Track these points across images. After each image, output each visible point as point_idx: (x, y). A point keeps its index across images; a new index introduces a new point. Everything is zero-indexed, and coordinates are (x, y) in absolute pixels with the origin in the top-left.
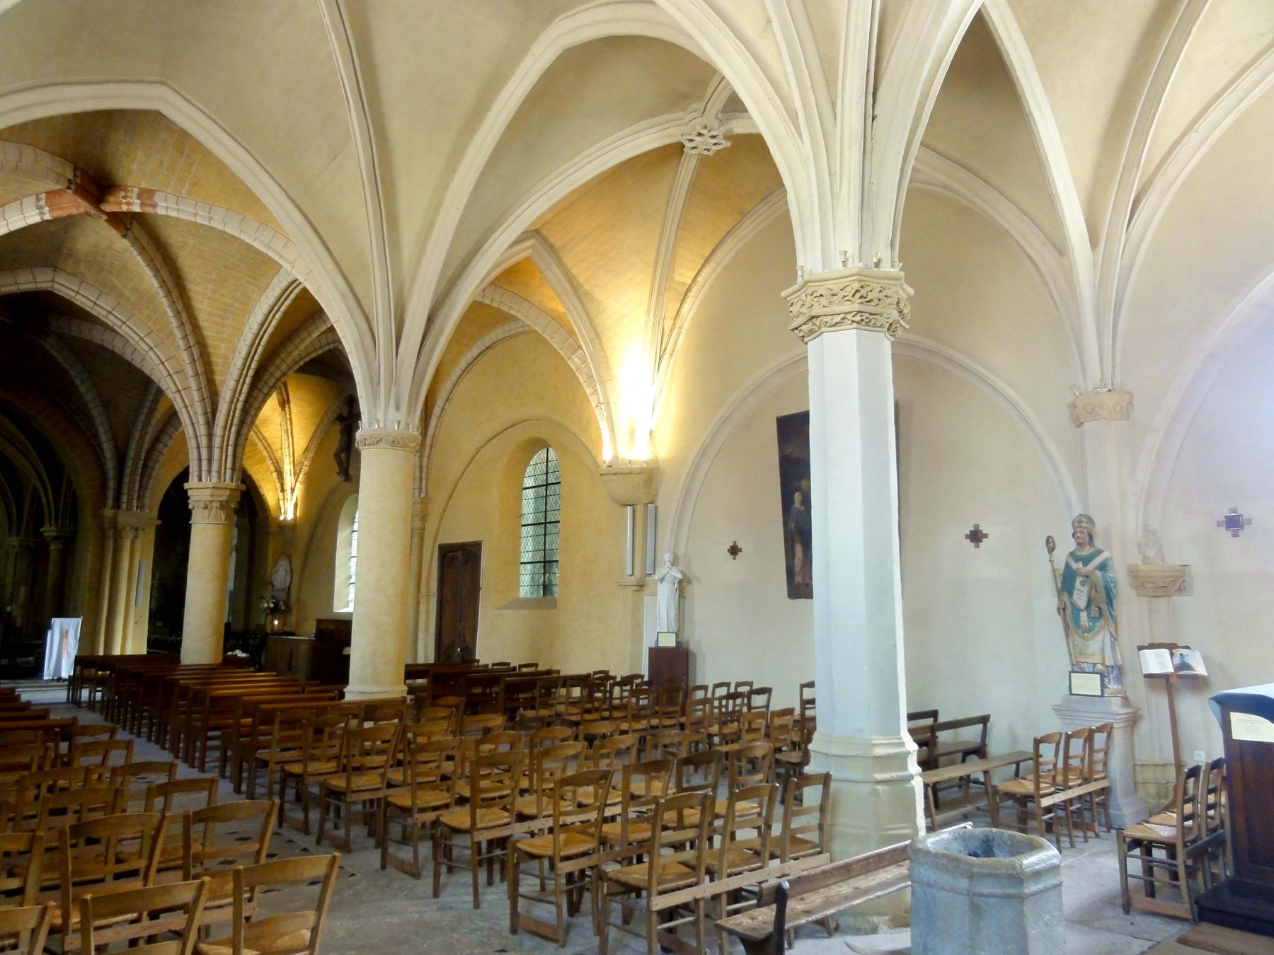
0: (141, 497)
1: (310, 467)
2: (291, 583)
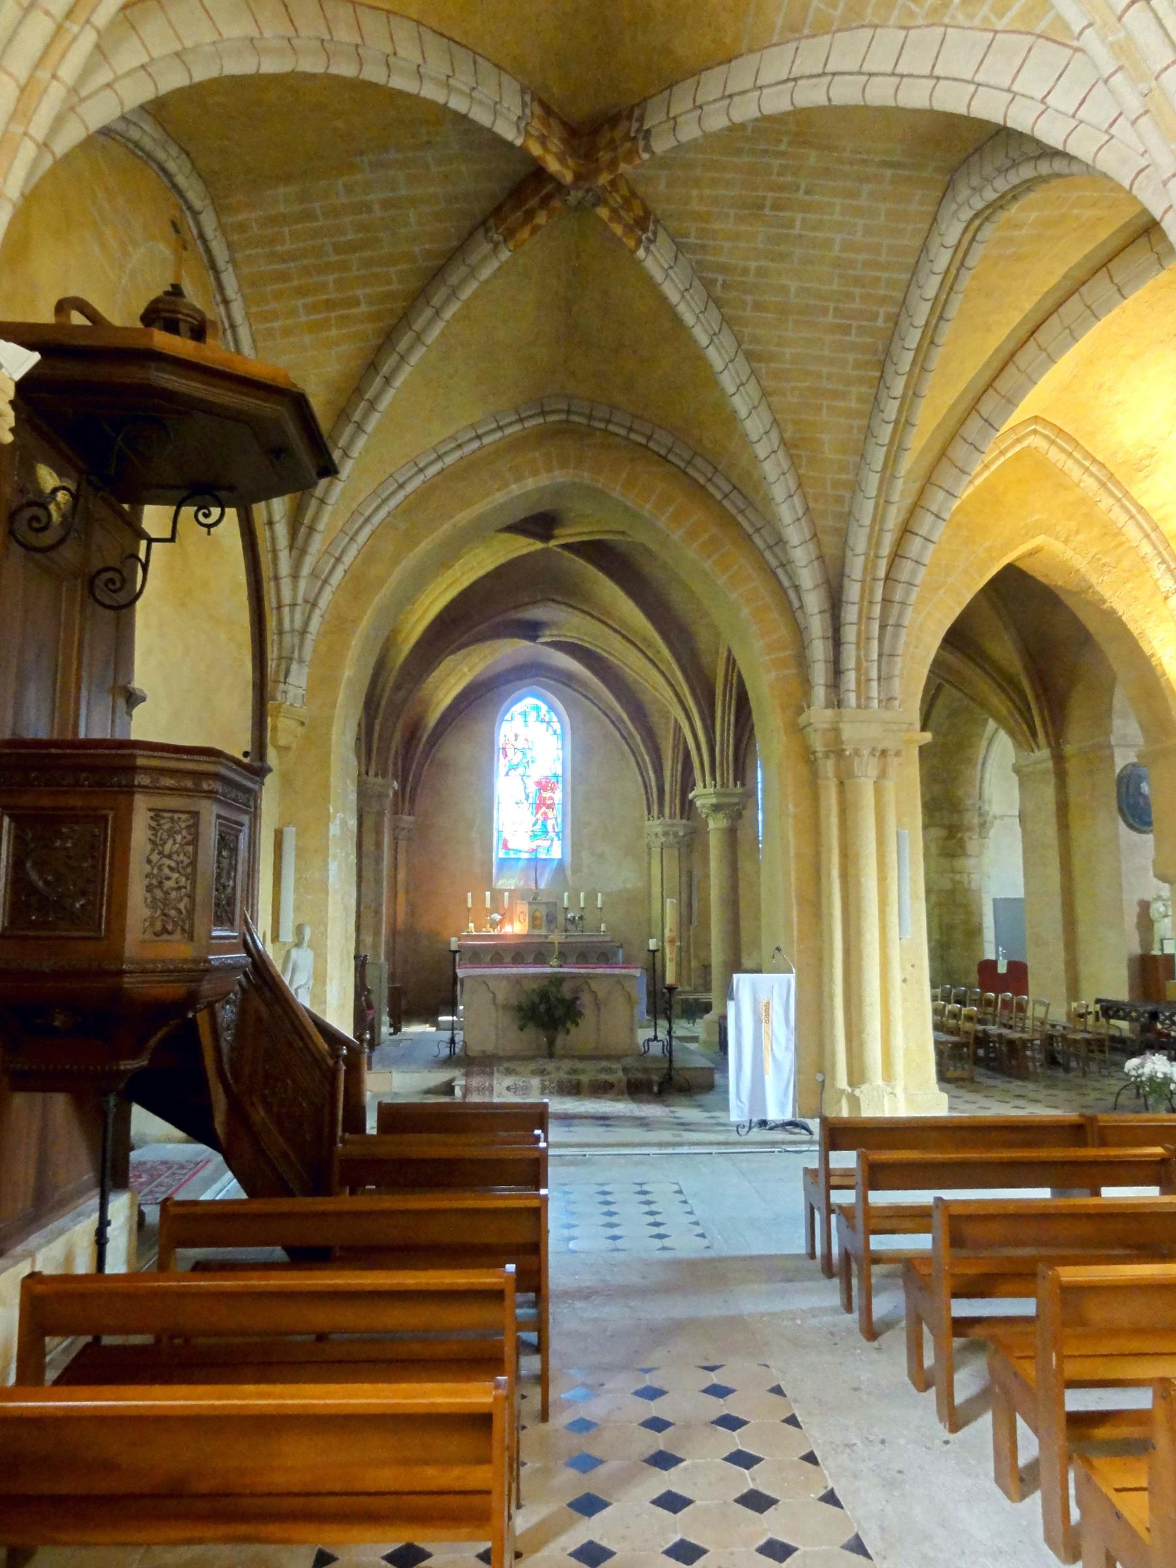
0: (884, 679)
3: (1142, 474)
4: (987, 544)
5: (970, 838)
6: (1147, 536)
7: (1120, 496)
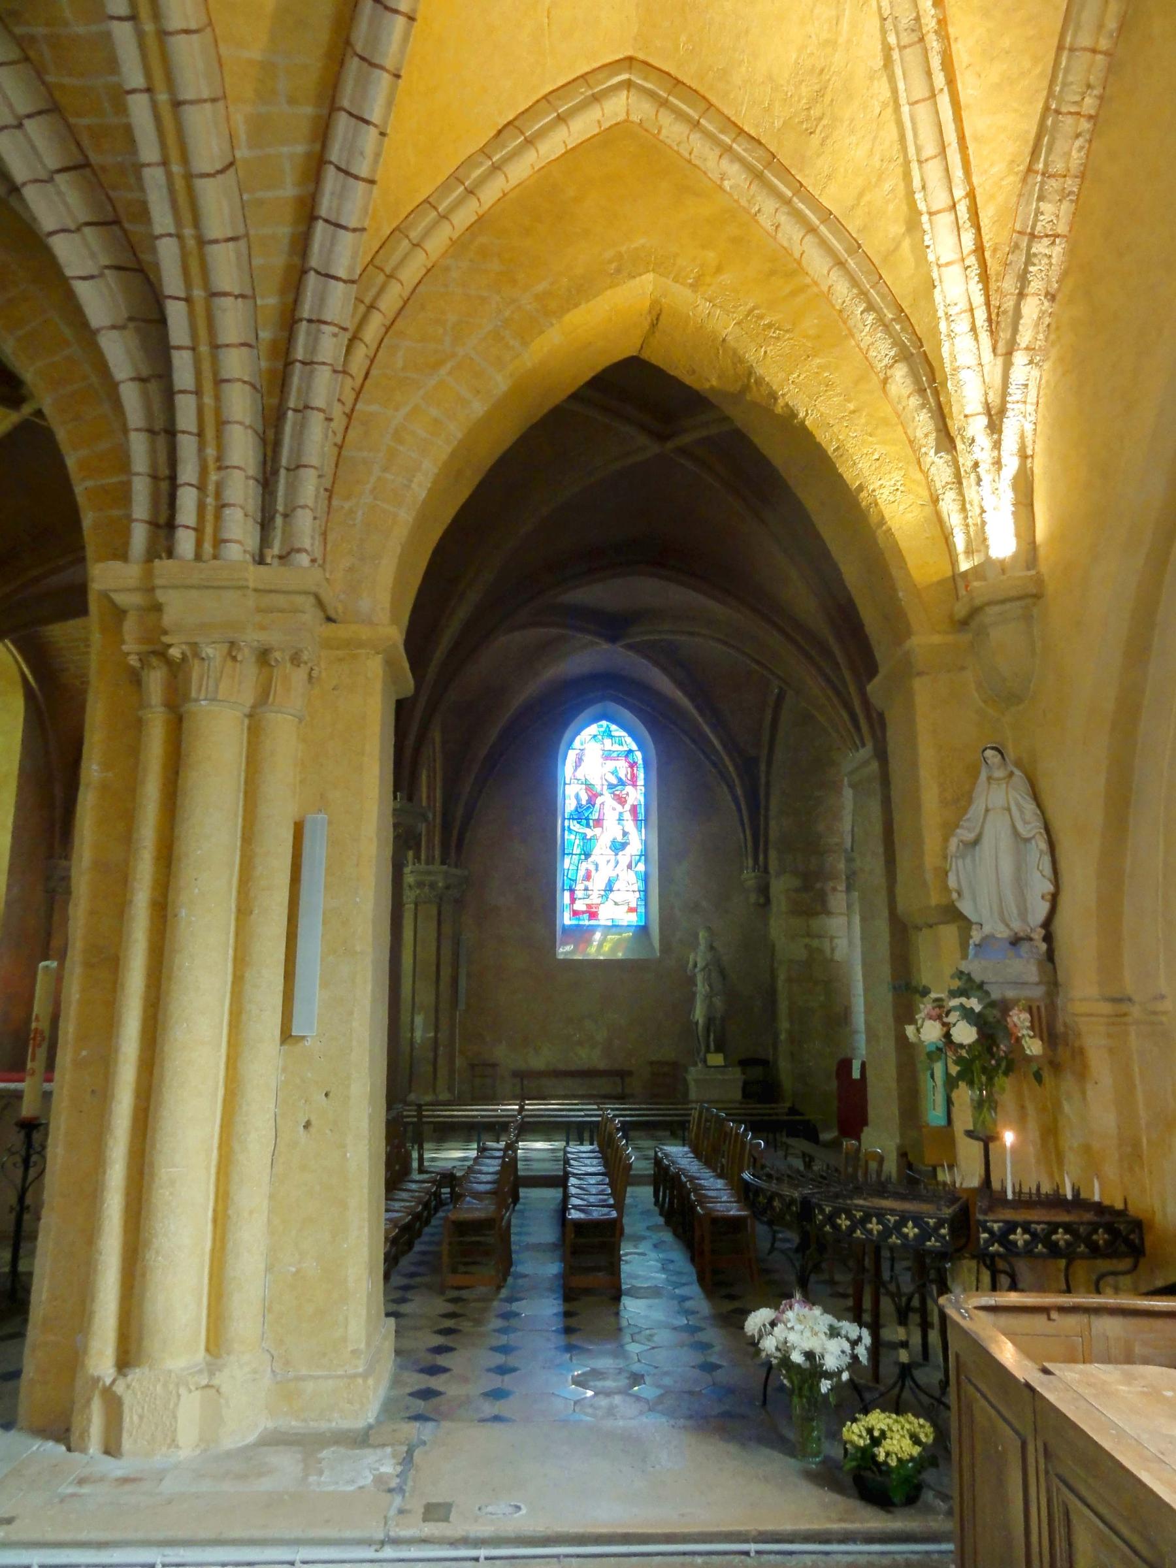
1: (1071, 253)
2: (1054, 899)
3: (815, 140)
4: (540, 287)
5: (834, 889)
6: (841, 264)
7: (789, 194)
